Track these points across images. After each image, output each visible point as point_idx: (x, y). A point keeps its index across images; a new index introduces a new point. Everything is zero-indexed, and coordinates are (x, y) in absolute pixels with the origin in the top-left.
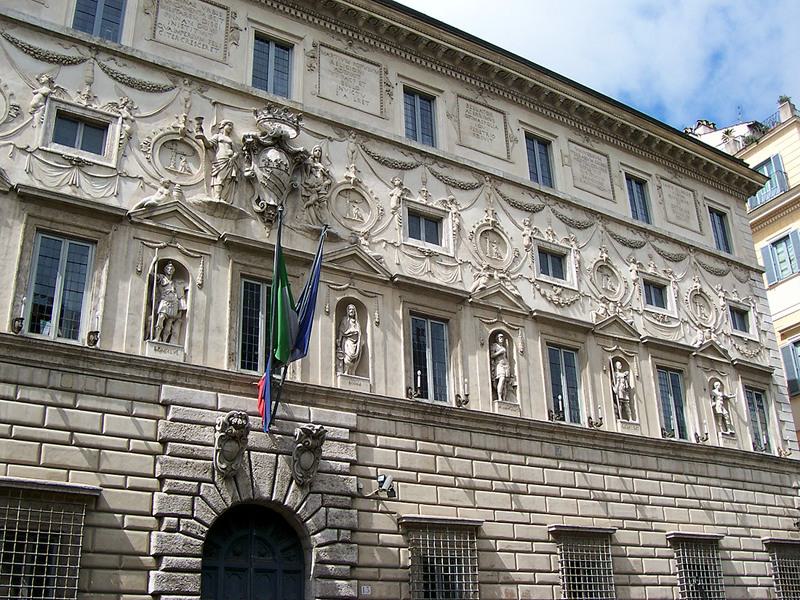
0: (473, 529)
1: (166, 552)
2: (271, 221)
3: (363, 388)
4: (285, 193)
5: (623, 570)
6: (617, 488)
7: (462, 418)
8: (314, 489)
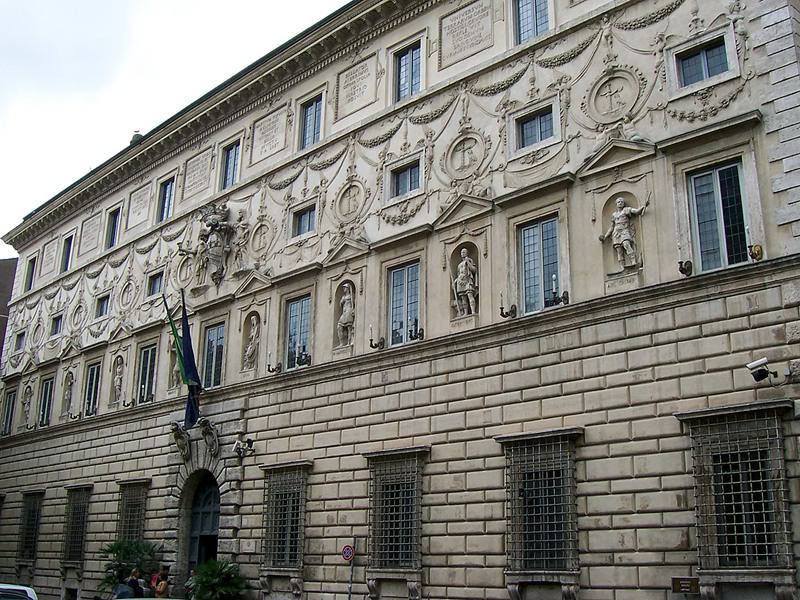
5: (440, 489)
6: (444, 399)
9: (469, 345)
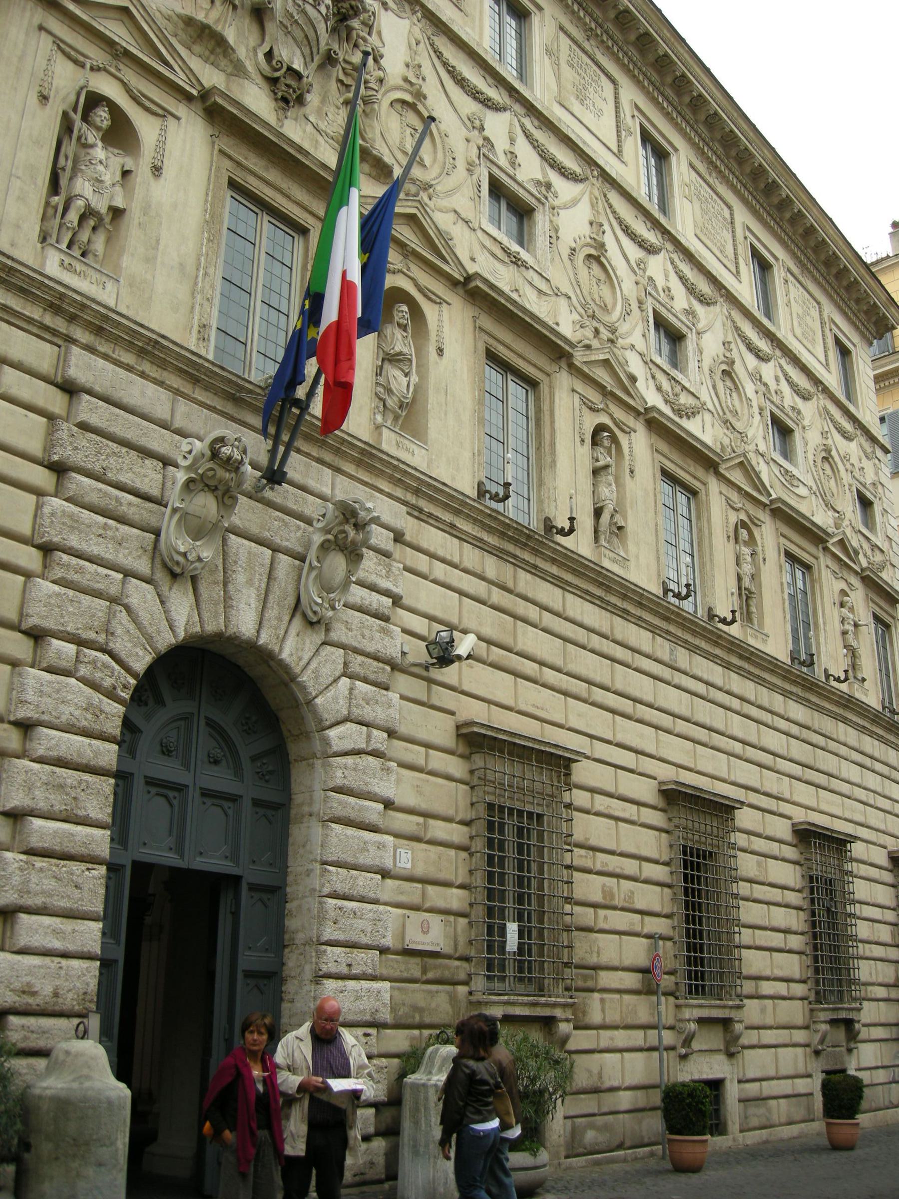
0: (559, 763)
1: (45, 717)
2: (285, 100)
3: (415, 457)
4: (317, 58)
7: (554, 561)
8: (334, 636)
9: (757, 671)
